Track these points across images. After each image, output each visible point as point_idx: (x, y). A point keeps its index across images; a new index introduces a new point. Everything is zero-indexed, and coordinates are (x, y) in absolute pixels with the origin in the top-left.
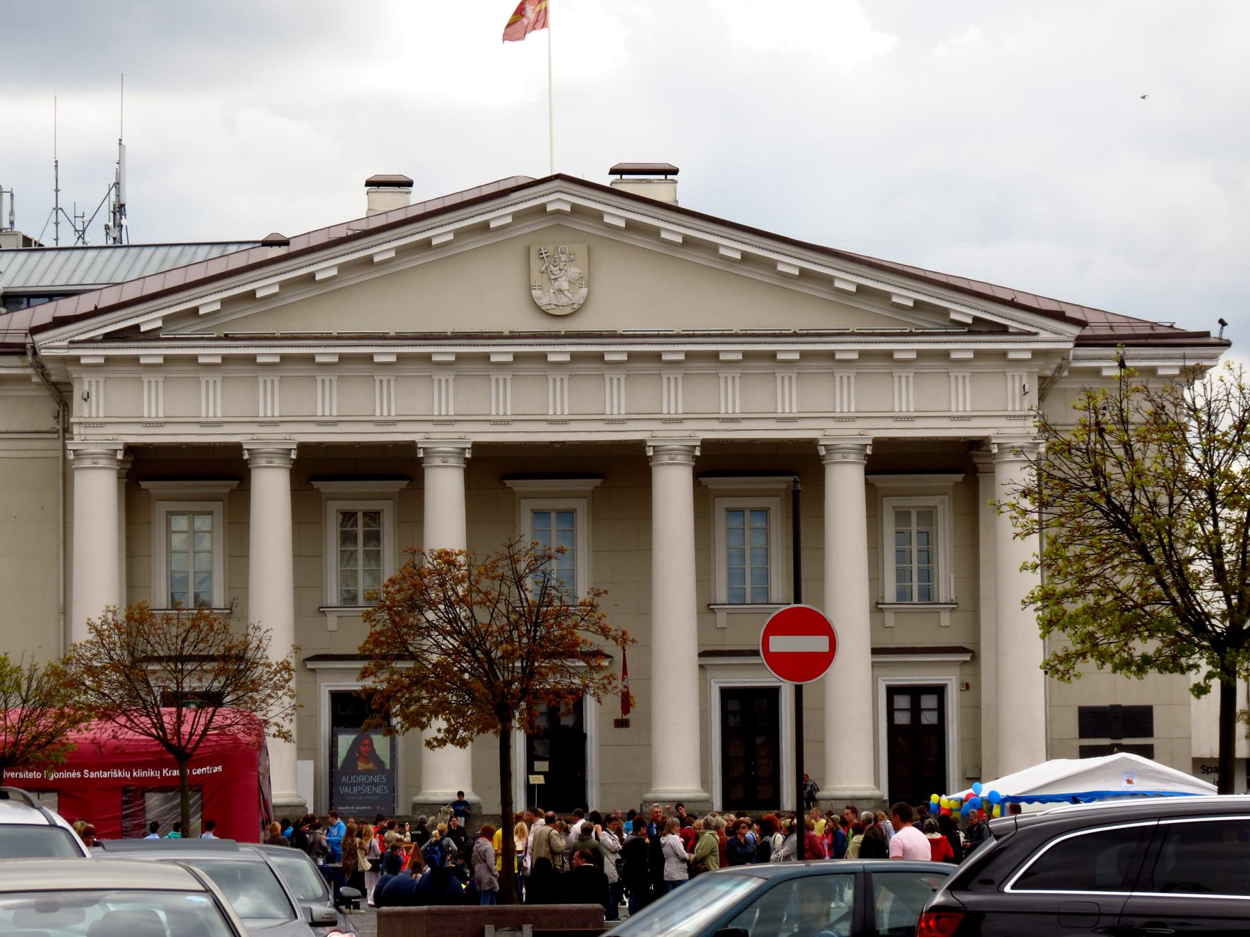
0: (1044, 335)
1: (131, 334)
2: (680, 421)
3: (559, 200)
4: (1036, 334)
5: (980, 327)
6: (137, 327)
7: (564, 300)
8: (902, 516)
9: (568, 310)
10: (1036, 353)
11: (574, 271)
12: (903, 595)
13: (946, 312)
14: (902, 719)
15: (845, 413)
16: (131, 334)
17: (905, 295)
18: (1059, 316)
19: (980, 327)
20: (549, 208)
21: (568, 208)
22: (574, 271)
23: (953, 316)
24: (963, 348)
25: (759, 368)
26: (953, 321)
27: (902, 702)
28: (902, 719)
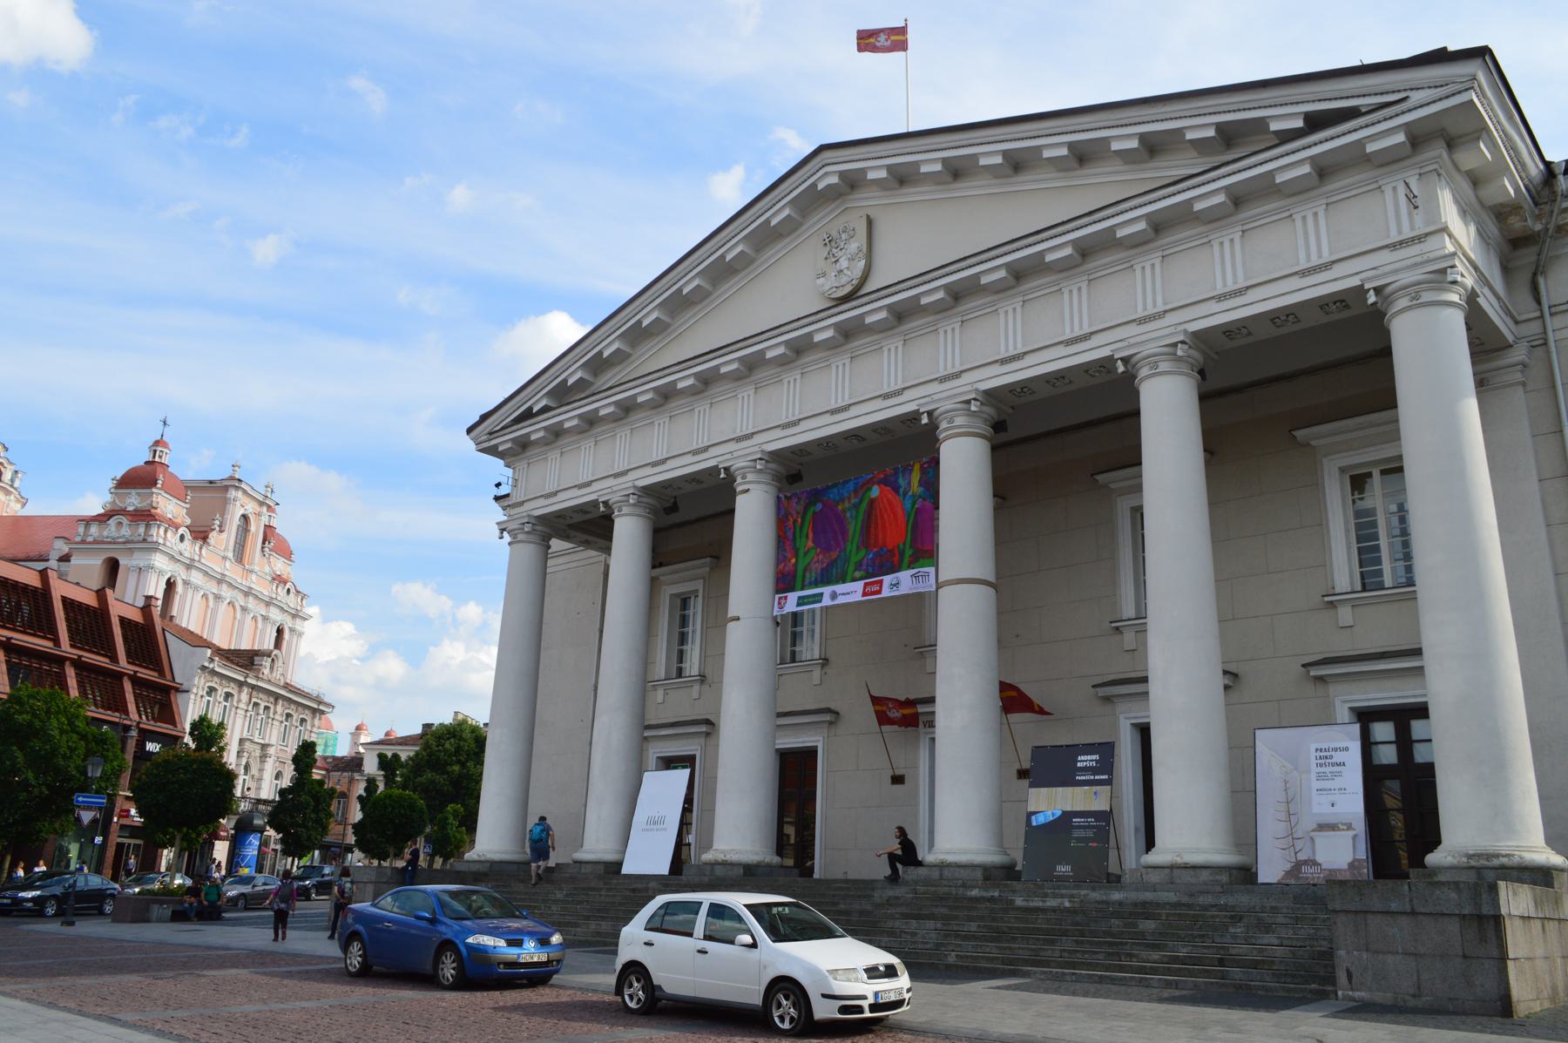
0: (1416, 97)
1: (528, 415)
2: (957, 375)
3: (826, 174)
4: (1406, 98)
5: (1315, 122)
6: (530, 408)
7: (844, 280)
8: (1359, 482)
9: (848, 289)
10: (1418, 138)
11: (853, 247)
12: (1370, 581)
13: (1261, 123)
14: (1387, 755)
15: (1147, 314)
16: (528, 415)
17: (1201, 128)
18: (1440, 57)
19: (1315, 122)
20: (820, 186)
21: (834, 180)
22: (853, 247)
23: (1274, 126)
24: (1291, 164)
25: (1039, 288)
26: (1276, 133)
27: (1383, 731)
28: (1387, 755)
